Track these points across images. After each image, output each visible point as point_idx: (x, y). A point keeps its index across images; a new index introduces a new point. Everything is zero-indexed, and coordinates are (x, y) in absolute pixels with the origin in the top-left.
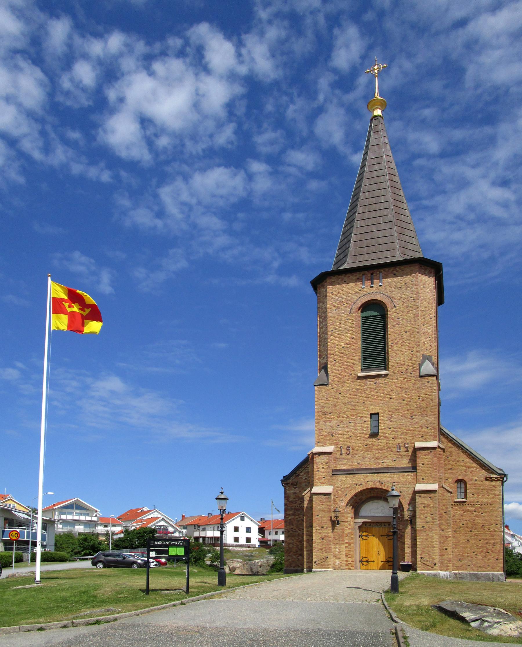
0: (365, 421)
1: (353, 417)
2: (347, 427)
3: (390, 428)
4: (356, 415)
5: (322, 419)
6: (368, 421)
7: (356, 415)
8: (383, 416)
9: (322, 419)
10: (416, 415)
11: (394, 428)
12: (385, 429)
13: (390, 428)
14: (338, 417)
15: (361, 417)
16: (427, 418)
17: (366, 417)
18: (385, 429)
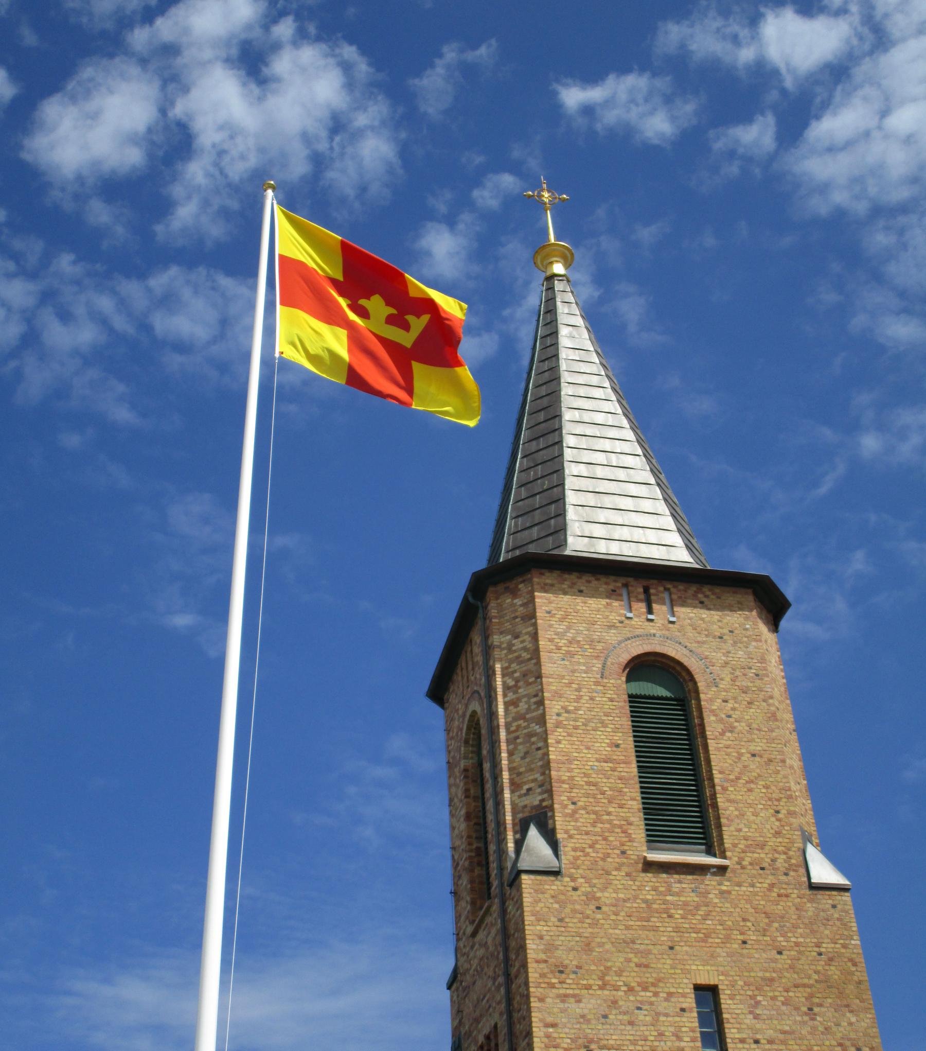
0: (683, 1010)
1: (645, 989)
2: (631, 1023)
3: (757, 1042)
4: (653, 985)
5: (552, 986)
6: (691, 1011)
7: (653, 985)
8: (732, 997)
9: (552, 986)
10: (821, 1005)
11: (770, 1042)
12: (742, 1041)
13: (757, 1042)
14: (602, 988)
15: (670, 994)
16: (853, 1019)
17: (684, 995)
18: (742, 1041)
